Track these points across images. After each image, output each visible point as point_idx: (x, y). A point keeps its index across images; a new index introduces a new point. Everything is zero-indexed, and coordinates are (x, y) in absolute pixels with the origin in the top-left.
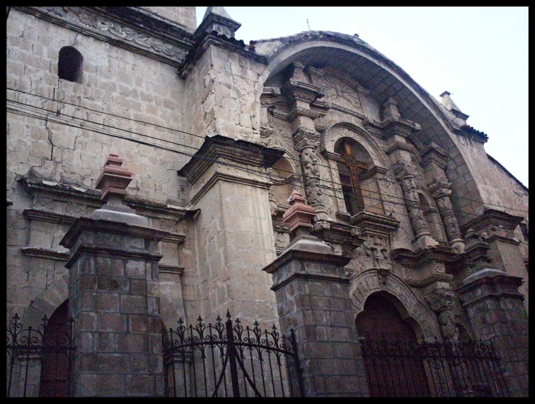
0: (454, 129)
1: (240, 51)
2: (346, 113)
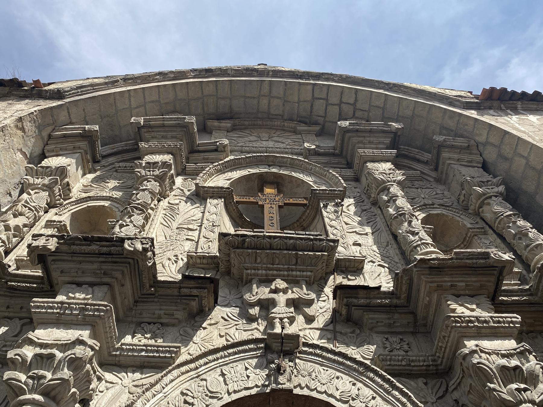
1: (18, 93)
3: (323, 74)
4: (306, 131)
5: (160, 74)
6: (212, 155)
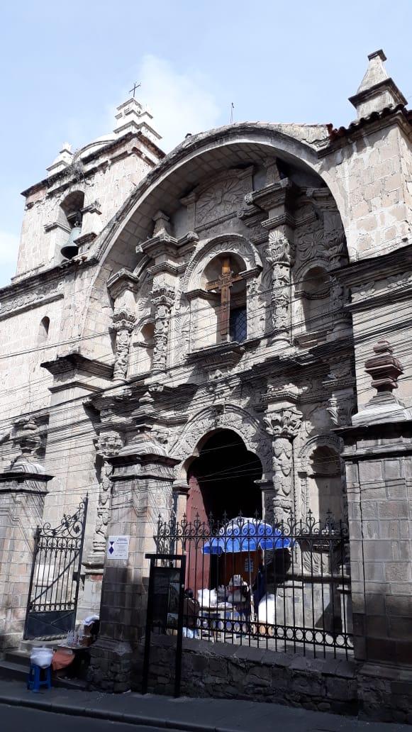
0: (319, 152)
3: (229, 130)
4: (244, 175)
5: (133, 196)
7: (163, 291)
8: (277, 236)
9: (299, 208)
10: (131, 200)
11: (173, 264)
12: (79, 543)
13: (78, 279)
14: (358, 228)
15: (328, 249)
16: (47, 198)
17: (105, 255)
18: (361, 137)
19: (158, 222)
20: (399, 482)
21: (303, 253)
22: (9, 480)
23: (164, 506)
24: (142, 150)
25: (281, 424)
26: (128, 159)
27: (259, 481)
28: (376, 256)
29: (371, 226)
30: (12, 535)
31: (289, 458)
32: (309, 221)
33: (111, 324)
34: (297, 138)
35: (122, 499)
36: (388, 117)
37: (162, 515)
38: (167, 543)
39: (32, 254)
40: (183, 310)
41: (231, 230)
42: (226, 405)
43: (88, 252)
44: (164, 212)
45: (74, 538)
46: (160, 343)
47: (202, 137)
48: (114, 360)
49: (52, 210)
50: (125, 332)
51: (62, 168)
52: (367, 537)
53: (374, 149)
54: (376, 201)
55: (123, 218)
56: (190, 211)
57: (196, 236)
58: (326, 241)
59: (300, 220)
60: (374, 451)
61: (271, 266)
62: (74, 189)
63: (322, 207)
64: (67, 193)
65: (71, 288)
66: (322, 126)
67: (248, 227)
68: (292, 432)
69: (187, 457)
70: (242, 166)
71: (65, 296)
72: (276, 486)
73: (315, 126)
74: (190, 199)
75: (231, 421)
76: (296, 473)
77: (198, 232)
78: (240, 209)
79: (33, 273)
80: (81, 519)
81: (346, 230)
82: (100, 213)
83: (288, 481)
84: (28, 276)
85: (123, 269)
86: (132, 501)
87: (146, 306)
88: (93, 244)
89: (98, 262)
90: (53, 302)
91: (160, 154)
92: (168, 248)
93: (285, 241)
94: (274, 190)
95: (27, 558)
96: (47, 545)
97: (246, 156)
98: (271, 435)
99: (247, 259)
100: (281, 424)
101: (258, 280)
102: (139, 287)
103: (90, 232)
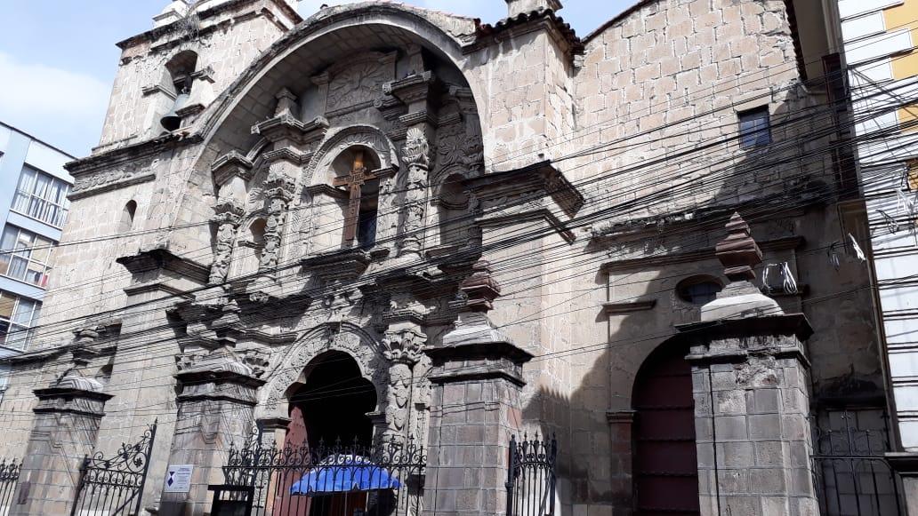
0: (464, 47)
2: (358, 110)
3: (371, 7)
6: (316, 134)
7: (279, 182)
8: (415, 134)
9: (444, 106)
10: (249, 71)
11: (293, 150)
12: (140, 479)
13: (176, 159)
14: (496, 137)
15: (467, 155)
16: (150, 54)
17: (212, 133)
18: (509, 38)
19: (282, 101)
20: (478, 406)
21: (443, 157)
22: (54, 398)
23: (240, 433)
24: (274, 13)
25: (401, 347)
26: (256, 20)
27: (371, 414)
28: (511, 169)
29: (509, 137)
30: (50, 465)
31: (406, 387)
32: (453, 122)
33: (213, 216)
34: (442, 29)
35: (189, 423)
36: (535, 21)
37: (236, 443)
38: (237, 474)
39: (122, 120)
40: (303, 205)
41: (367, 120)
42: (343, 322)
43: (191, 127)
44: (289, 89)
45: (133, 473)
46: (271, 244)
47: (339, 10)
48: (212, 261)
49: (154, 69)
50: (228, 227)
51: (172, 19)
52: (443, 464)
53: (520, 53)
54: (517, 110)
55: (239, 92)
56: (322, 92)
57: (326, 122)
58: (467, 146)
59: (442, 120)
60: (459, 373)
61: (408, 166)
62: (185, 47)
63: (465, 109)
64: (175, 51)
65: (166, 168)
66: (469, 19)
67: (387, 119)
68: (413, 357)
69: (291, 383)
70: (385, 50)
71: (158, 178)
72: (388, 419)
73: (462, 18)
74: (322, 79)
75: (347, 342)
76: (413, 405)
77: (329, 118)
78: (378, 100)
79: (122, 145)
80: (145, 449)
81: (484, 138)
82: (212, 81)
83: (402, 413)
84: (115, 147)
85: (233, 152)
86: (200, 425)
87: (259, 198)
88: (198, 118)
89: (202, 140)
90: (143, 182)
91: (296, 19)
92: (291, 132)
93: (424, 141)
94: (416, 82)
95: (67, 495)
96: (96, 479)
97: (389, 40)
98: (388, 360)
99: (383, 156)
100: (401, 347)
101: (393, 181)
102: (252, 175)
103: (196, 103)
